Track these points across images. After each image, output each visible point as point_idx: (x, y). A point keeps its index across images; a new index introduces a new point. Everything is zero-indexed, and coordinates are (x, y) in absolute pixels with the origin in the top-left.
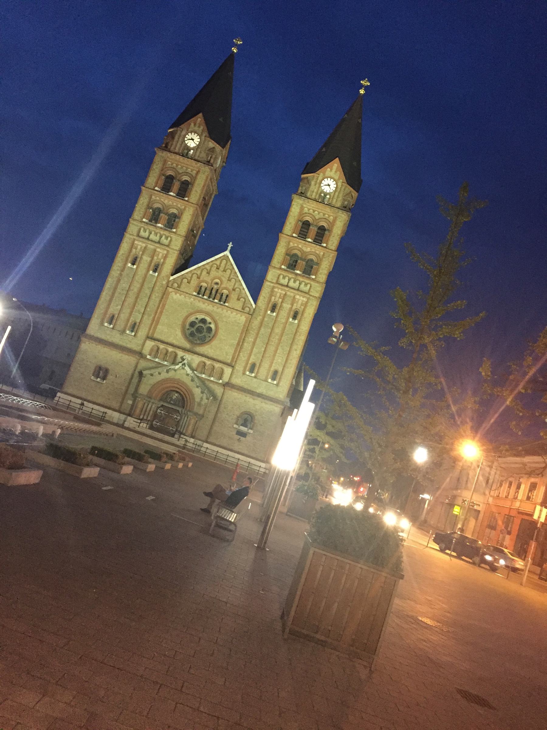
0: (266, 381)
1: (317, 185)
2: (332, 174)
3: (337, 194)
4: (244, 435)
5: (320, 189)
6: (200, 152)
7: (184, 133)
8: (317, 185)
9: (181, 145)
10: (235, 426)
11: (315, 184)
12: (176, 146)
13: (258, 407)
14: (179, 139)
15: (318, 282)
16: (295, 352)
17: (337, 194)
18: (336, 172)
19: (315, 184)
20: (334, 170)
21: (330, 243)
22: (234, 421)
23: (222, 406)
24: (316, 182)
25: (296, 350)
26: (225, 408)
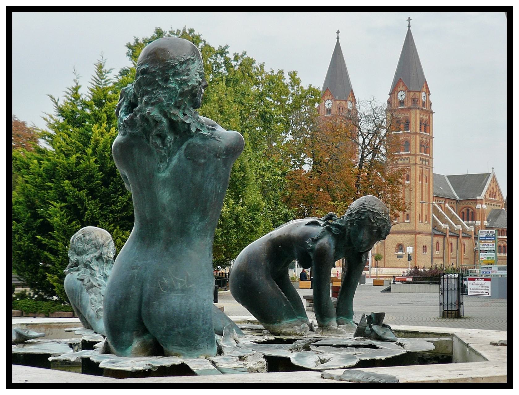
0: (404, 222)
1: (396, 98)
2: (401, 88)
3: (407, 98)
4: (400, 257)
5: (398, 100)
6: (334, 109)
7: (323, 102)
8: (396, 98)
9: (324, 110)
10: (395, 253)
11: (394, 99)
12: (322, 111)
13: (403, 239)
14: (322, 107)
15: (412, 155)
16: (413, 200)
17: (407, 98)
18: (403, 87)
19: (394, 99)
20: (401, 86)
21: (412, 129)
22: (394, 251)
23: (386, 245)
24: (394, 97)
25: (413, 199)
26: (388, 246)
